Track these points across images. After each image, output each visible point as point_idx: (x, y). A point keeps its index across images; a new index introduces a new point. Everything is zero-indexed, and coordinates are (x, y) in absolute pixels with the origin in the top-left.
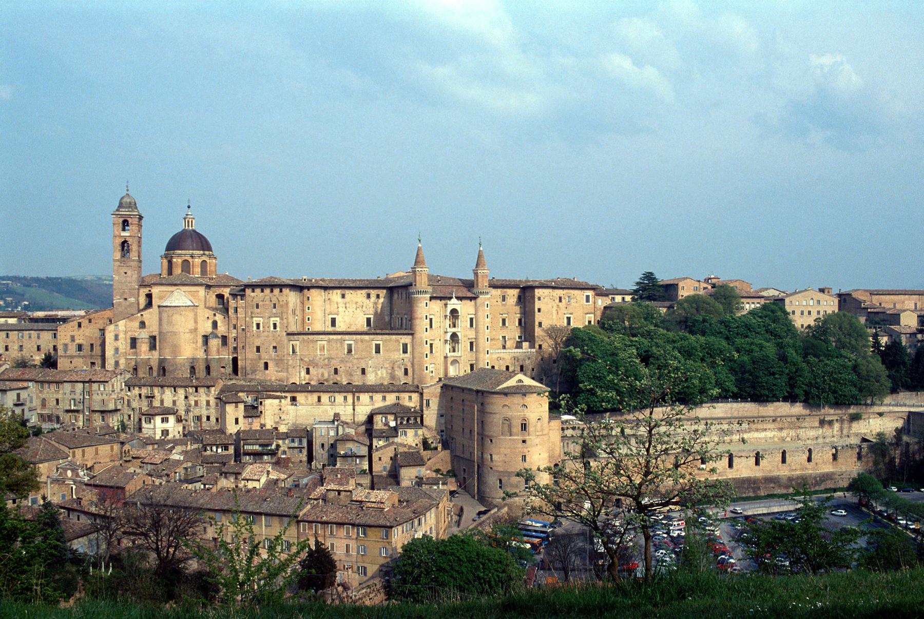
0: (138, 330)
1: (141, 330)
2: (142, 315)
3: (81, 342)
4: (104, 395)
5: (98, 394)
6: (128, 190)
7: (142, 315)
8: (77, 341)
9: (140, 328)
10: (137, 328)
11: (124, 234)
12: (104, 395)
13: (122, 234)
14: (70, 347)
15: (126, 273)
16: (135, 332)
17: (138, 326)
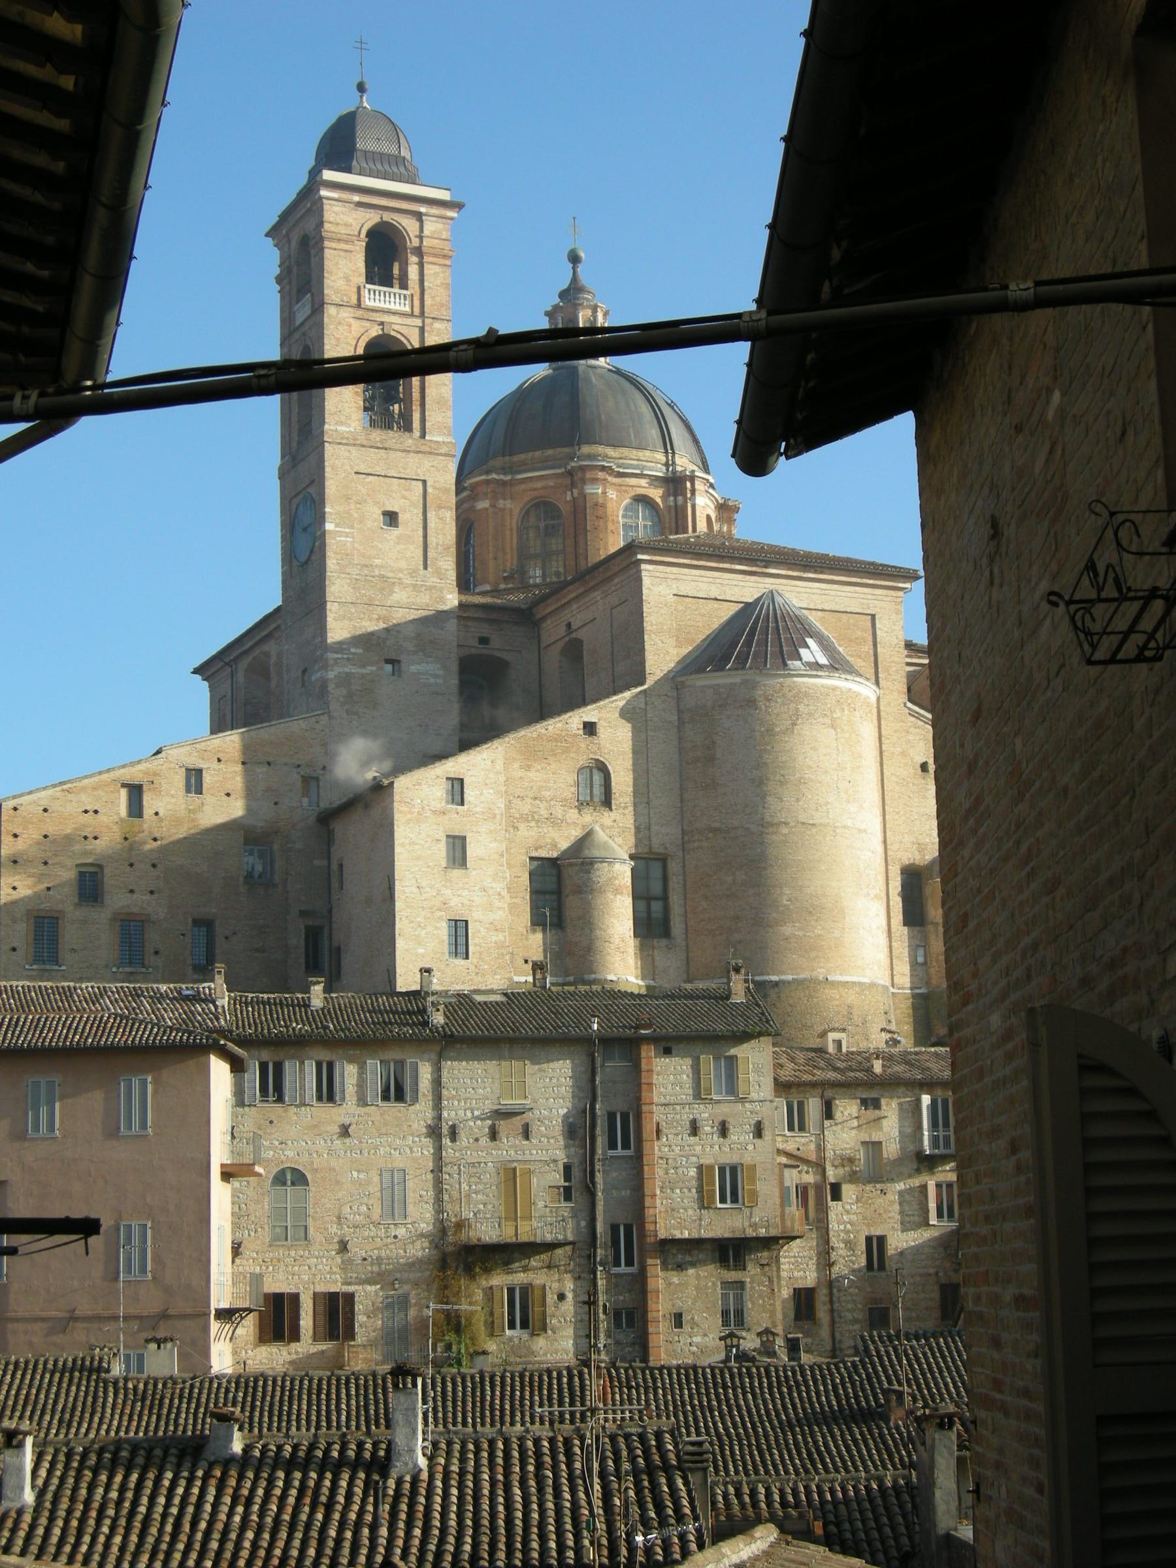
0: (573, 814)
1: (588, 817)
2: (590, 728)
3: (141, 902)
4: (740, 1135)
5: (694, 1129)
6: (361, 88)
7: (590, 728)
8: (117, 900)
9: (581, 805)
10: (564, 802)
11: (380, 299)
12: (740, 1135)
13: (368, 302)
14: (70, 936)
15: (391, 518)
16: (553, 821)
17: (570, 792)
